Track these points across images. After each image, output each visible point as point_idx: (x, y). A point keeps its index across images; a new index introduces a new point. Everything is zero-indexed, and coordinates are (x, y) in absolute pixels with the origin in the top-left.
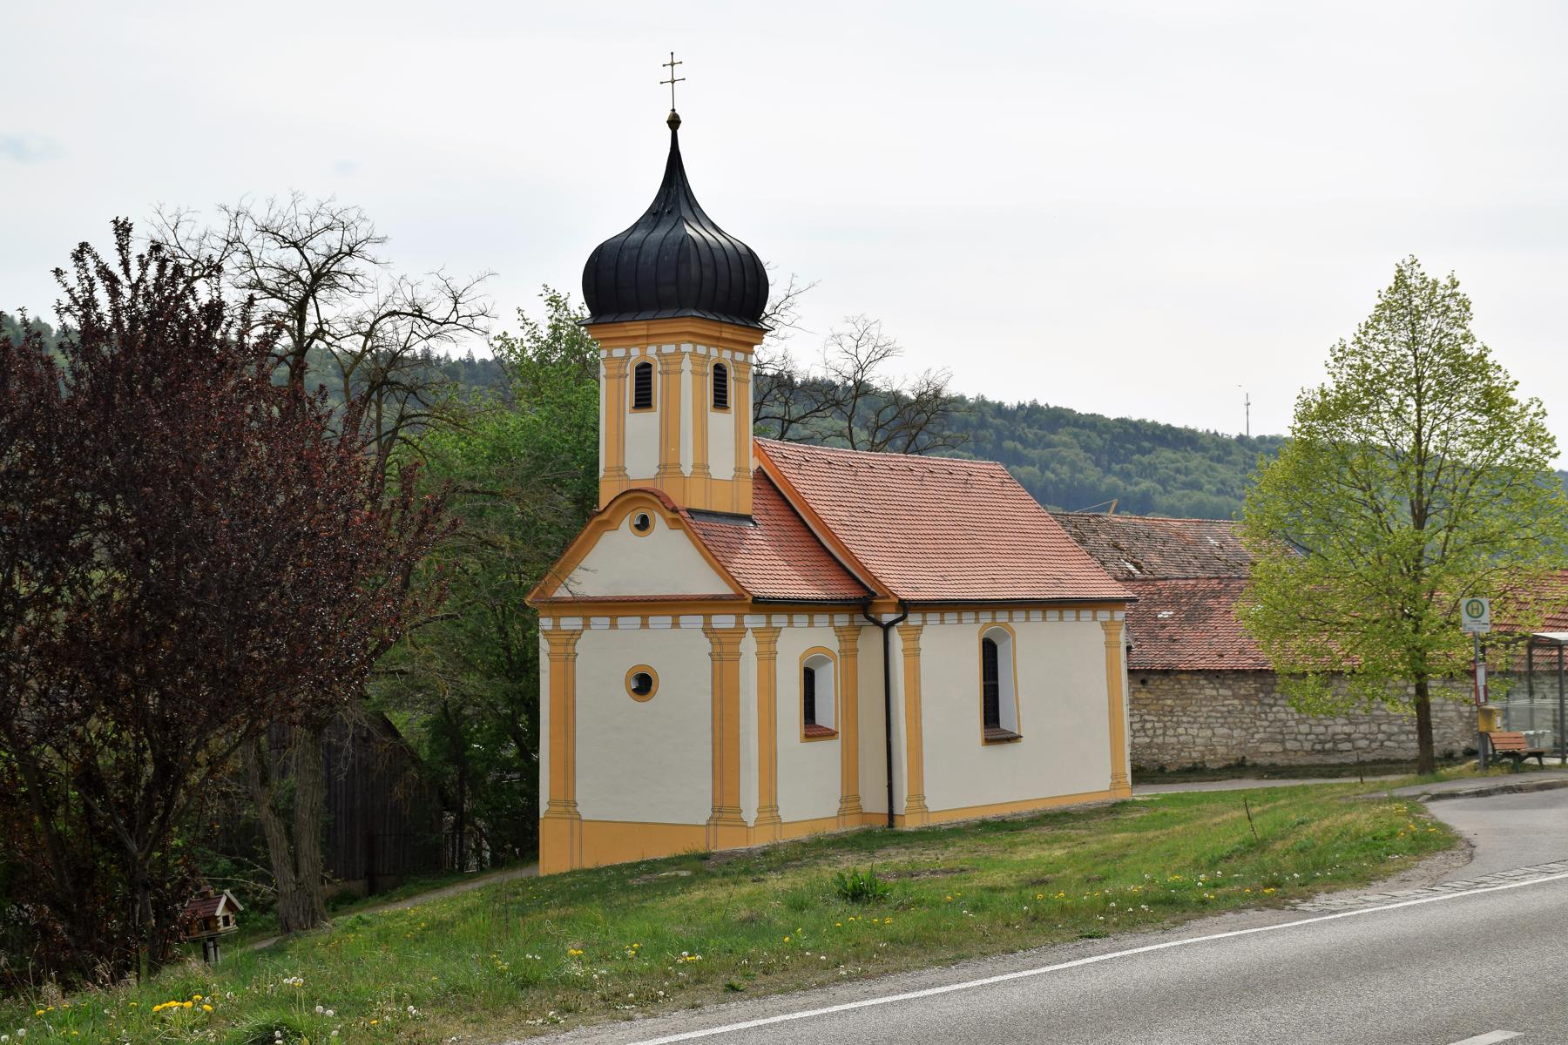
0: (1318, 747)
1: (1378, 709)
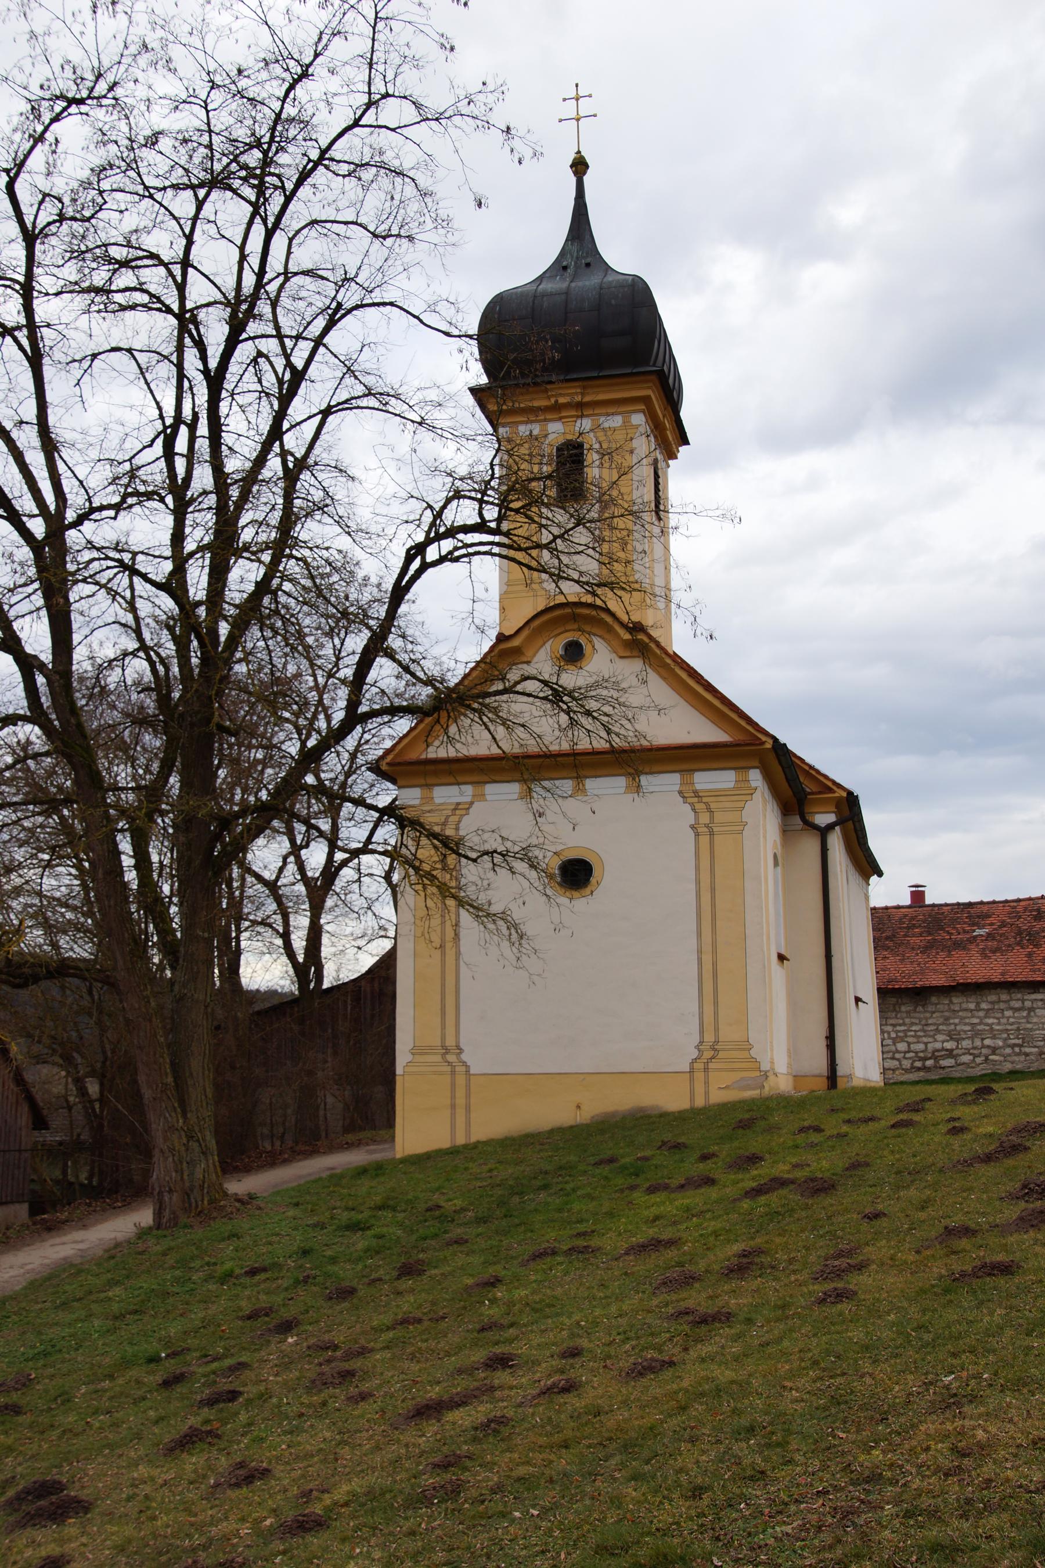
0: (918, 1064)
1: (980, 1024)
